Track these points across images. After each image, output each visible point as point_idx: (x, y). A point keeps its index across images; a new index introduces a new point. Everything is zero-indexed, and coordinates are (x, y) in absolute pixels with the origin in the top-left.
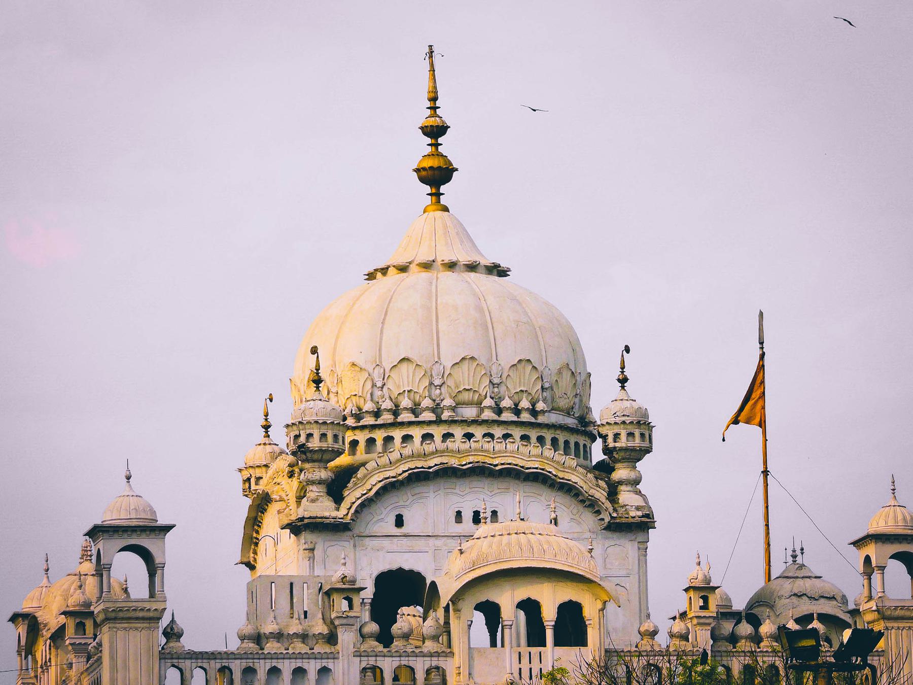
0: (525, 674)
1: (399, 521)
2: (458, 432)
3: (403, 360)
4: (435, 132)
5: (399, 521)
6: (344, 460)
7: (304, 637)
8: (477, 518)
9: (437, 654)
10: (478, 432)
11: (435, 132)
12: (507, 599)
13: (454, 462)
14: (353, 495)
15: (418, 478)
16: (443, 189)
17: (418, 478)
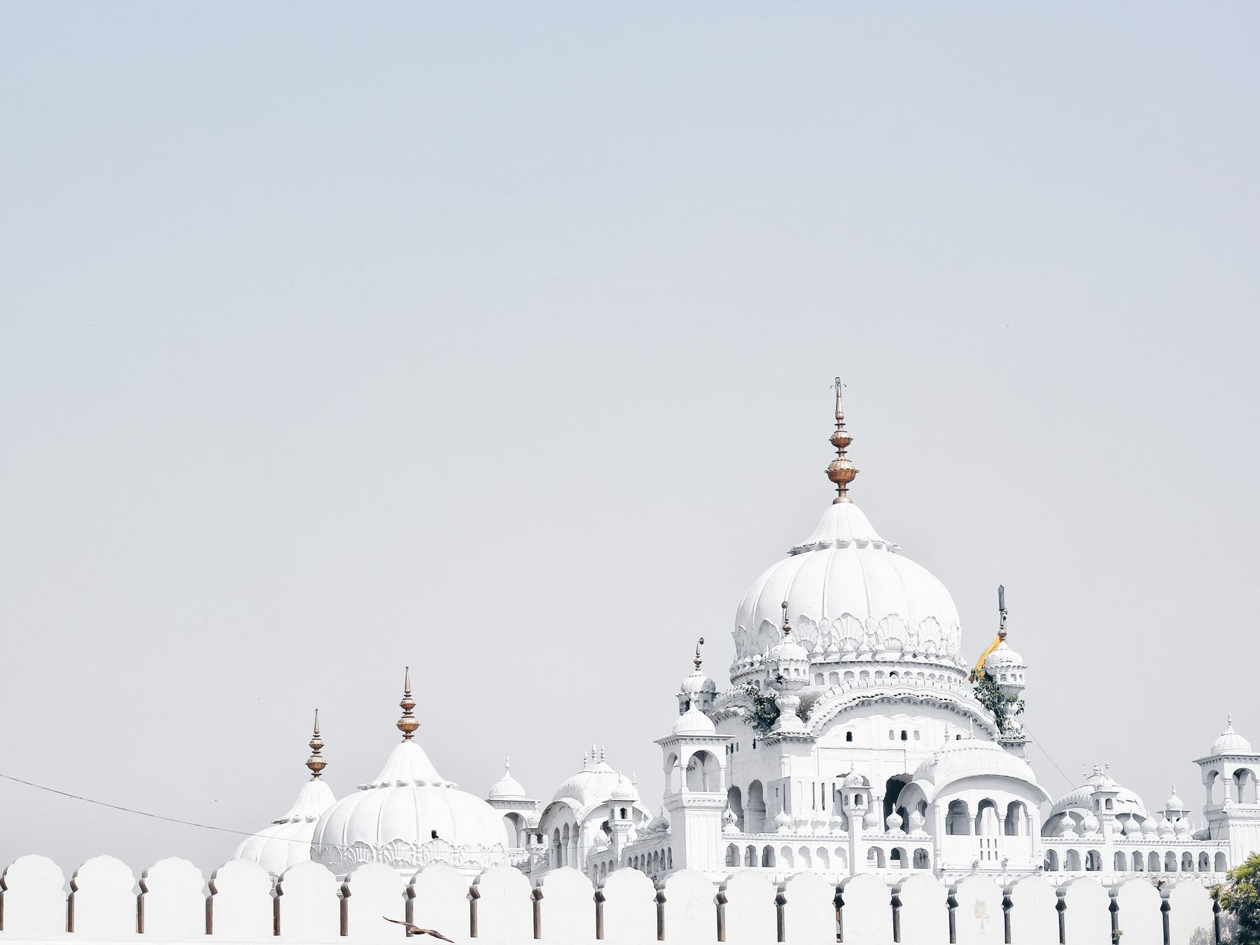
0: (985, 855)
1: (849, 737)
2: (887, 670)
3: (845, 615)
4: (840, 444)
5: (849, 737)
6: (808, 691)
7: (816, 824)
8: (904, 736)
9: (920, 840)
10: (901, 670)
11: (840, 444)
12: (971, 798)
13: (889, 693)
14: (815, 715)
15: (865, 703)
16: (848, 486)
17: (865, 703)
